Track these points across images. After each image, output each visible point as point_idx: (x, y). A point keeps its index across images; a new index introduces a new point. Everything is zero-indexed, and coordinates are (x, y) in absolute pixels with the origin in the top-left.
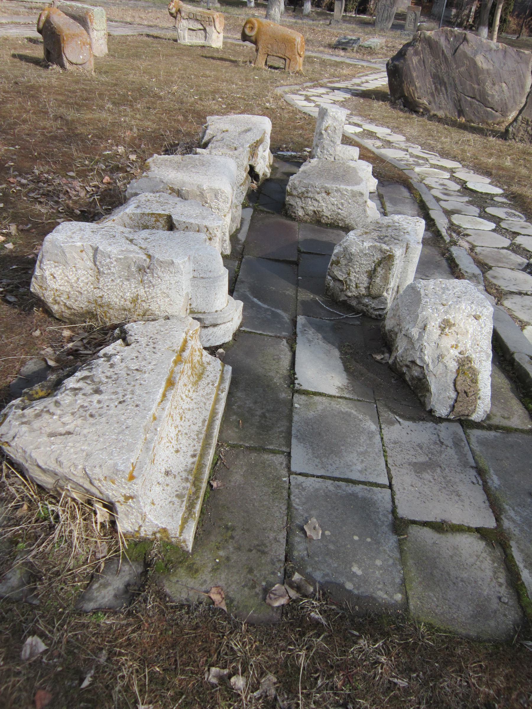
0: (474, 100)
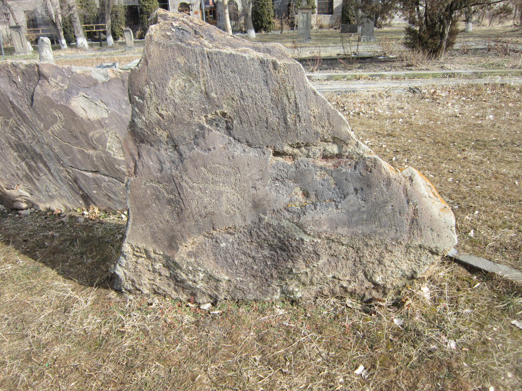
0: (99, 175)
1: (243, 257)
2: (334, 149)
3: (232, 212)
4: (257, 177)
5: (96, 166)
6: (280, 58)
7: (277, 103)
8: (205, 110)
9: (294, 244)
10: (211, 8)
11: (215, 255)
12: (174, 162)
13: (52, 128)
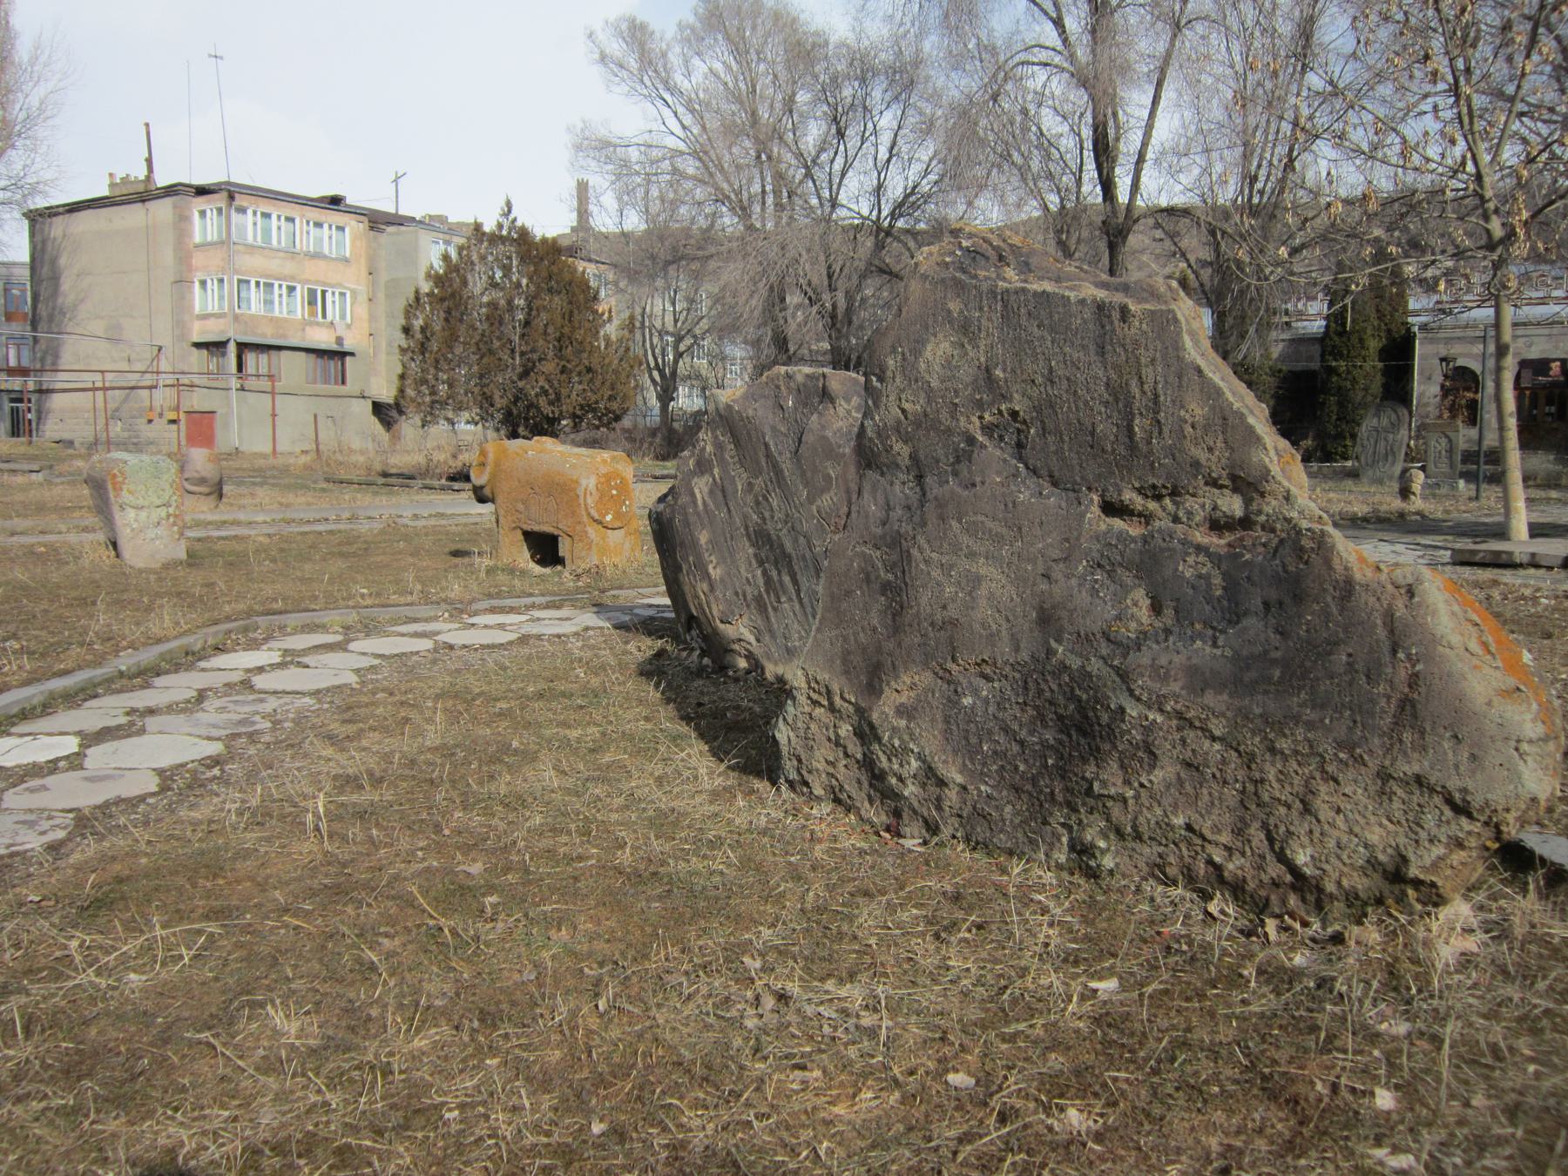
1: (1001, 738)
2: (1233, 505)
3: (994, 627)
4: (1056, 554)
6: (1141, 301)
7: (1118, 395)
8: (980, 405)
9: (1105, 718)
10: (1554, 384)
11: (947, 720)
12: (909, 508)
13: (819, 502)
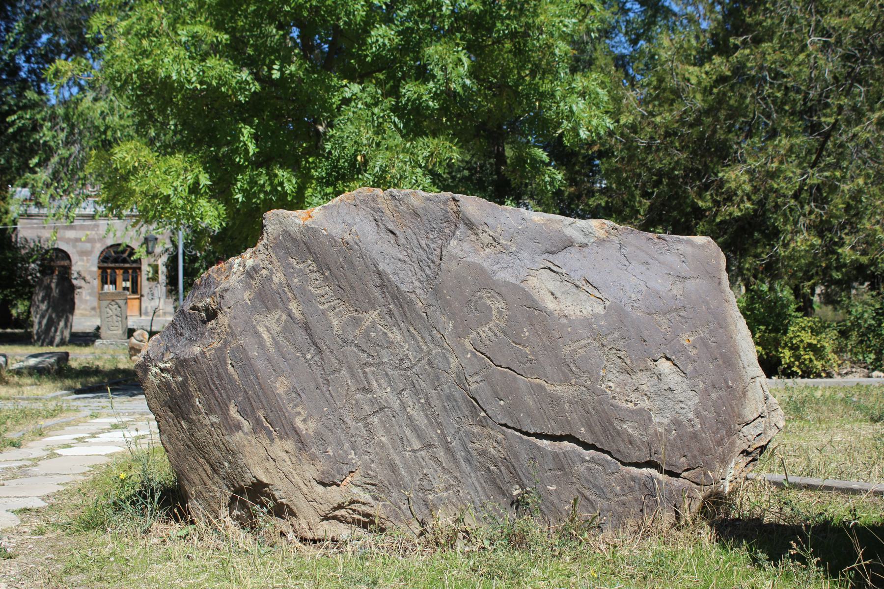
5: (568, 422)
